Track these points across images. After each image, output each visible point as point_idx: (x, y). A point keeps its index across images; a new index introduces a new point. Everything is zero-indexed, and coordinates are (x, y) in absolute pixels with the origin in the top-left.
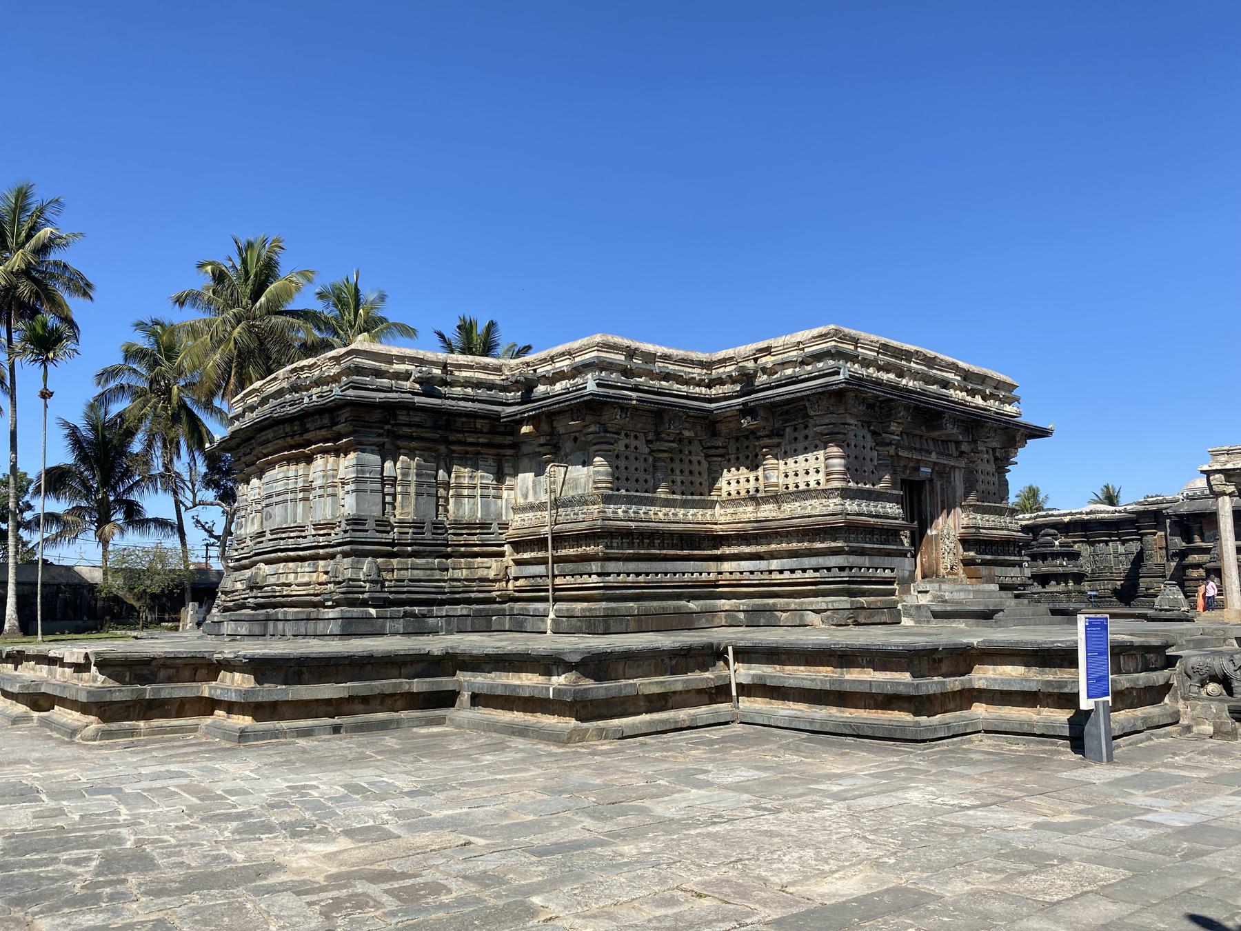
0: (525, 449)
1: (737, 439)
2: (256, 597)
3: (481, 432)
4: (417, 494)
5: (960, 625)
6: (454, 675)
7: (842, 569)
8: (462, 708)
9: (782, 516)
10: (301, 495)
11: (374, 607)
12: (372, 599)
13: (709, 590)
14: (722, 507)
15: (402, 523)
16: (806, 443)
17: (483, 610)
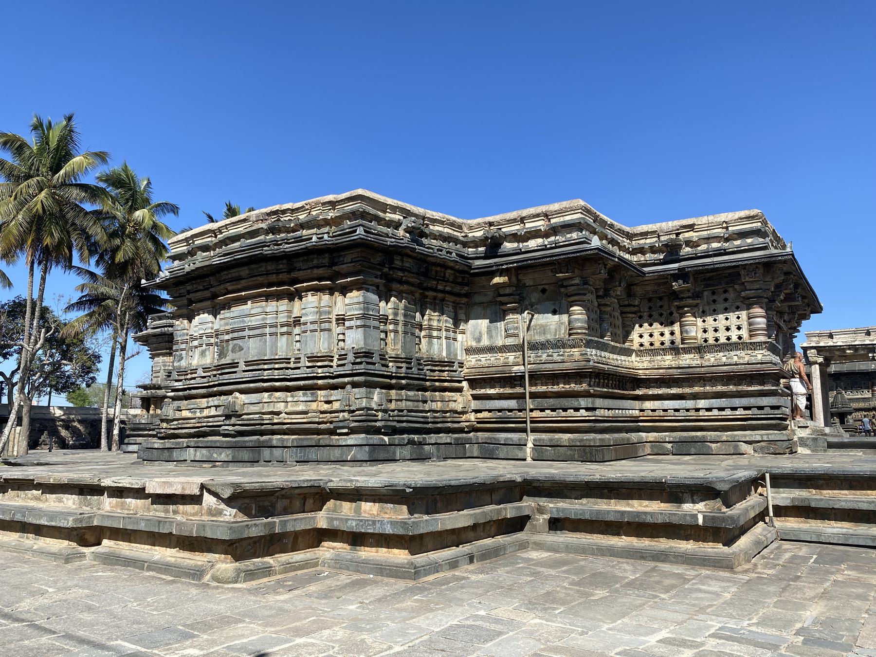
0: (478, 299)
1: (650, 300)
2: (234, 425)
3: (447, 281)
4: (405, 333)
5: (859, 453)
6: (521, 500)
7: (773, 408)
8: (535, 531)
9: (707, 364)
10: (285, 329)
11: (385, 434)
12: (385, 427)
13: (633, 425)
14: (637, 355)
15: (396, 359)
16: (727, 305)
17: (460, 438)
